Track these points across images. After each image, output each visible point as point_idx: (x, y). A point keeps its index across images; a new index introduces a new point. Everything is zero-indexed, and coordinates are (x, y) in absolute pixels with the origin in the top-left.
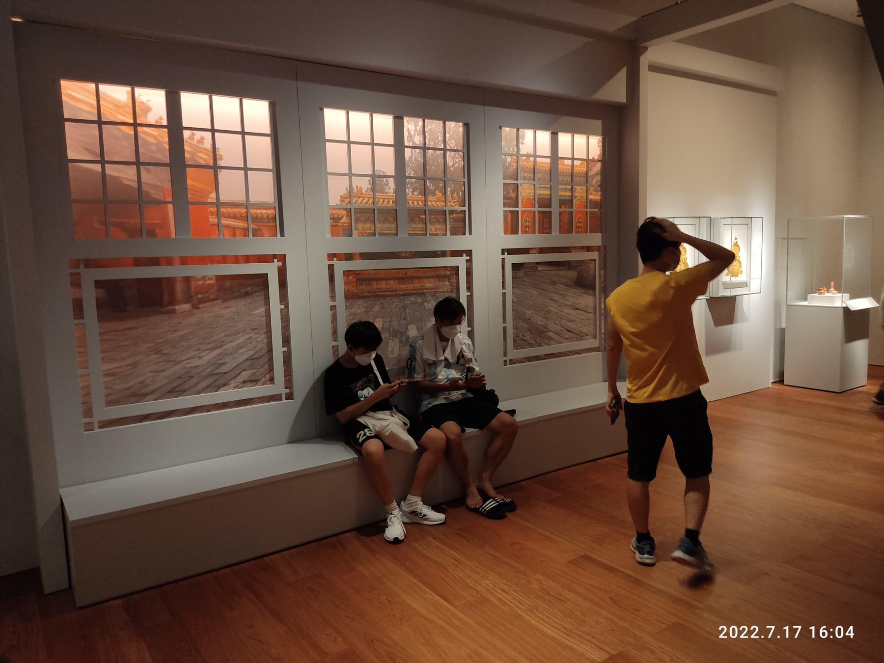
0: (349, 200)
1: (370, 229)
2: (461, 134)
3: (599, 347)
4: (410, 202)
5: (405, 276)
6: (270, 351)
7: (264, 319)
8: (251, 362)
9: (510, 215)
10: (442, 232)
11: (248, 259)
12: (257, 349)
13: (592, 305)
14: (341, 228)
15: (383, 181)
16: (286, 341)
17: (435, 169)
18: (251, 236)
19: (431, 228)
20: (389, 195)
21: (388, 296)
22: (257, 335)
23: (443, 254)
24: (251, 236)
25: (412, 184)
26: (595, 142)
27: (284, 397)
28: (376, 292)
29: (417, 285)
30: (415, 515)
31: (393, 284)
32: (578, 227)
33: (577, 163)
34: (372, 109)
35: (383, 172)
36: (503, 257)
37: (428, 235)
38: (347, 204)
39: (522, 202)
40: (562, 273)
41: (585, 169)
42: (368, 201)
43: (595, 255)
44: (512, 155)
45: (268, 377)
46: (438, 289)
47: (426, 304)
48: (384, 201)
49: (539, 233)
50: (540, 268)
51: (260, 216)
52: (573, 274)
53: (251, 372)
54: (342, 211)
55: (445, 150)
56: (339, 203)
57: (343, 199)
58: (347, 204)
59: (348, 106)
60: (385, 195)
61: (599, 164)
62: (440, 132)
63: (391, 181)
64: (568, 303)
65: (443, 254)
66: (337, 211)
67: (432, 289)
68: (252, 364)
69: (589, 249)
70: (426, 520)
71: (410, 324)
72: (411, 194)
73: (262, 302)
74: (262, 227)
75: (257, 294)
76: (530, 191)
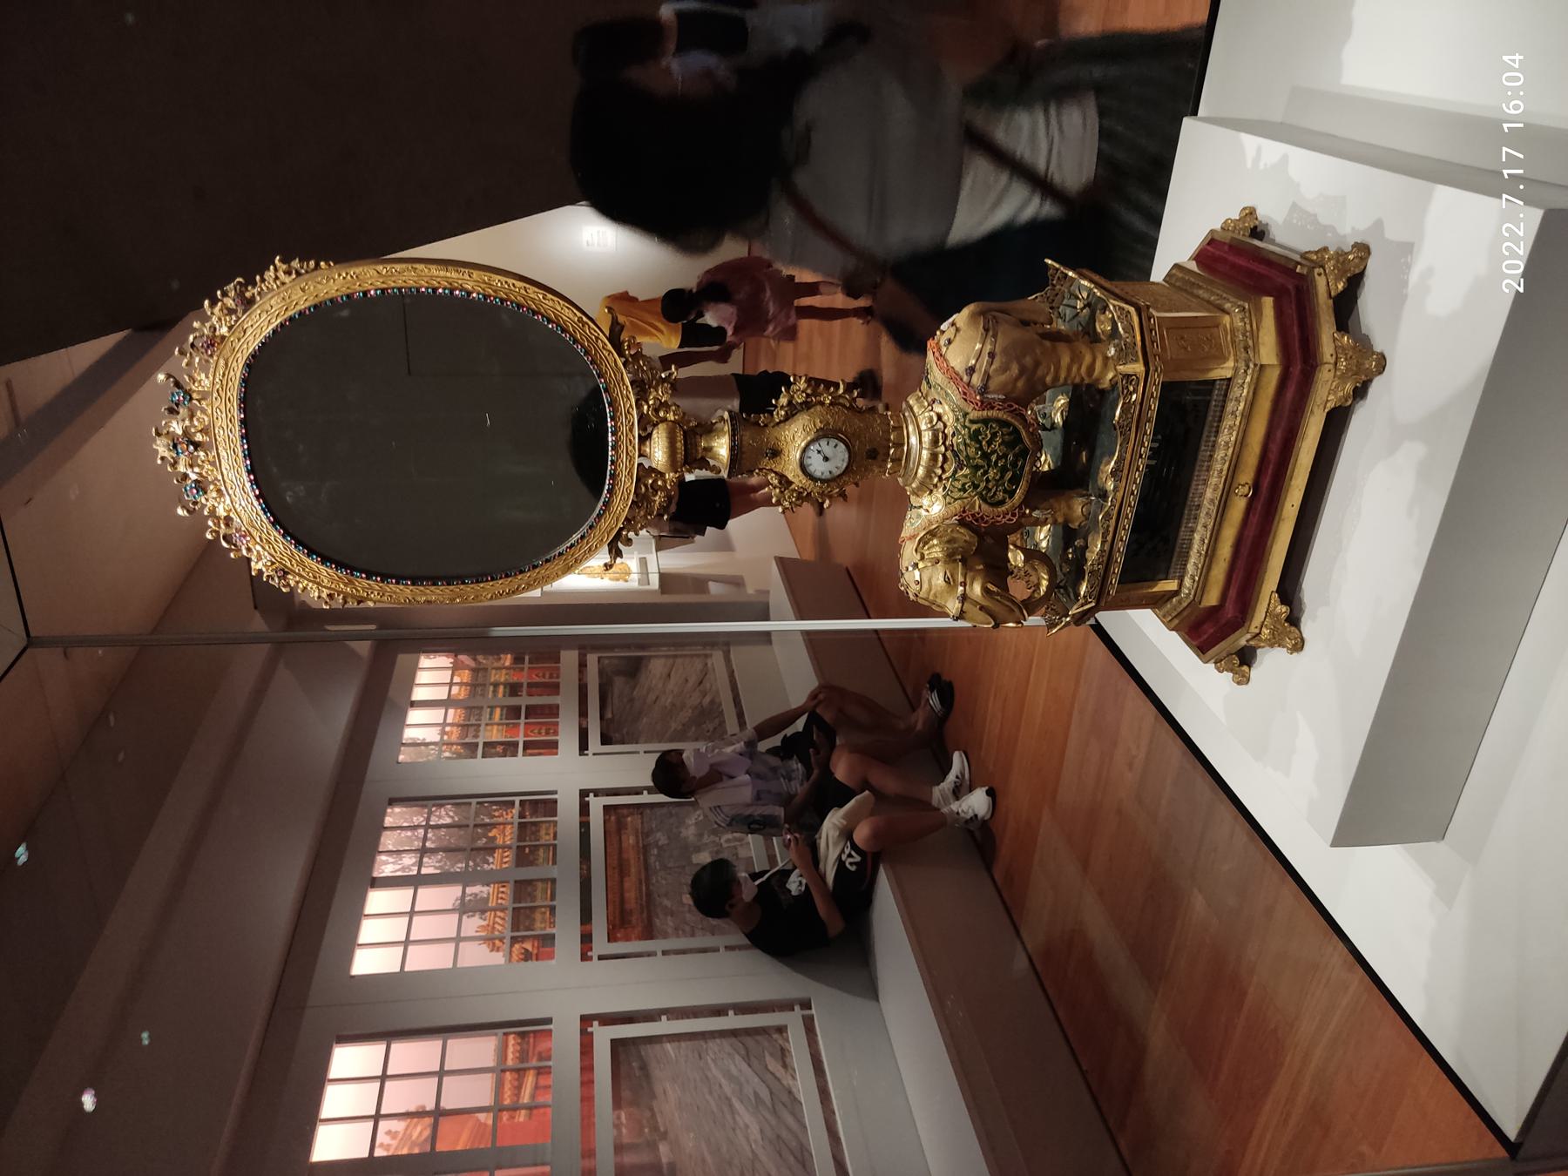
0: (497, 942)
1: (545, 913)
2: (404, 809)
3: (724, 652)
4: (504, 866)
5: (617, 867)
6: (734, 1033)
7: (683, 1044)
8: (752, 1058)
9: (529, 751)
10: (552, 827)
11: (587, 1068)
12: (732, 1051)
13: (662, 661)
14: (541, 950)
15: (470, 900)
16: (719, 1011)
17: (453, 838)
18: (550, 1063)
19: (545, 839)
20: (491, 893)
21: (647, 888)
22: (710, 1052)
23: (585, 826)
24: (550, 1063)
25: (476, 865)
26: (425, 661)
27: (807, 1012)
28: (641, 905)
29: (631, 856)
30: (959, 791)
31: (630, 883)
32: (551, 677)
33: (457, 680)
34: (356, 915)
35: (457, 900)
36: (595, 958)
37: (556, 842)
38: (503, 943)
39: (511, 737)
40: (616, 691)
41: (467, 671)
42: (500, 917)
43: (592, 659)
44: (441, 751)
45: (776, 1036)
46: (637, 830)
47: (660, 843)
48: (502, 898)
49: (558, 717)
50: (609, 715)
51: (518, 1055)
52: (619, 683)
53: (768, 1058)
54: (514, 949)
55: (427, 827)
56: (501, 954)
57: (494, 949)
58: (503, 943)
59: (349, 944)
60: (491, 897)
61: (460, 657)
62: (400, 834)
63: (469, 890)
64: (660, 685)
65: (585, 826)
66: (514, 955)
67: (637, 837)
68: (755, 1057)
69: (582, 665)
70: (963, 775)
71: (691, 861)
72: (491, 866)
73: (657, 1047)
74: (536, 1052)
75: (643, 1053)
76: (495, 731)
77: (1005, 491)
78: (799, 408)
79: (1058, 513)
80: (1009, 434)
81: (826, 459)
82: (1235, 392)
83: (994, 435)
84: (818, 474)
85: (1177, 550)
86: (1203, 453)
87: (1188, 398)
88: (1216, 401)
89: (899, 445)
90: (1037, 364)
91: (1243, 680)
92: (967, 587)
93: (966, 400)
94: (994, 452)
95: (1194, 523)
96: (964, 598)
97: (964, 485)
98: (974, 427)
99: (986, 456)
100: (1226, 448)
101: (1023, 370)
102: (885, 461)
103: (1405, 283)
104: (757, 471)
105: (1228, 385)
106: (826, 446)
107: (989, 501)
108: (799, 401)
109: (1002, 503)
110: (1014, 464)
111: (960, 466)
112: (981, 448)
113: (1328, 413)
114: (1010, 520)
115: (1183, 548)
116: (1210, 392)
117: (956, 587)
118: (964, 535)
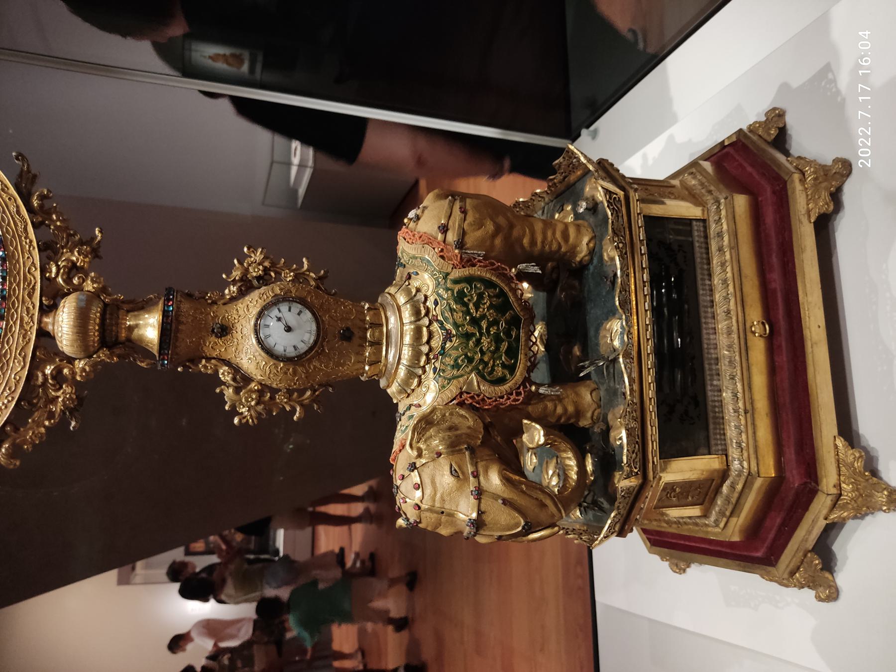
77: (504, 366)
78: (255, 282)
79: (566, 400)
80: (497, 296)
81: (288, 329)
82: (713, 228)
83: (480, 296)
84: (279, 349)
85: (711, 415)
86: (703, 299)
87: (671, 237)
88: (698, 241)
89: (377, 325)
90: (511, 226)
91: (833, 595)
92: (481, 478)
93: (442, 257)
94: (483, 317)
95: (719, 380)
96: (479, 493)
97: (456, 360)
98: (457, 288)
99: (475, 322)
100: (724, 286)
101: (498, 229)
102: (362, 347)
103: (838, 92)
104: (204, 361)
105: (705, 227)
106: (289, 313)
107: (488, 378)
108: (254, 274)
109: (501, 381)
110: (508, 334)
111: (448, 337)
112: (468, 312)
113: (814, 223)
114: (515, 400)
115: (716, 412)
116: (690, 233)
117: (466, 479)
118: (468, 421)
